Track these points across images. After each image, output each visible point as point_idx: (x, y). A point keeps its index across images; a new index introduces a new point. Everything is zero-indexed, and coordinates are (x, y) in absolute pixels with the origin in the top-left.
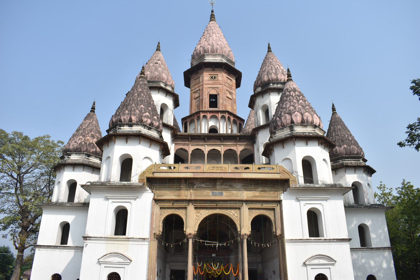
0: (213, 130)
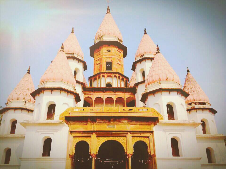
0: (109, 85)
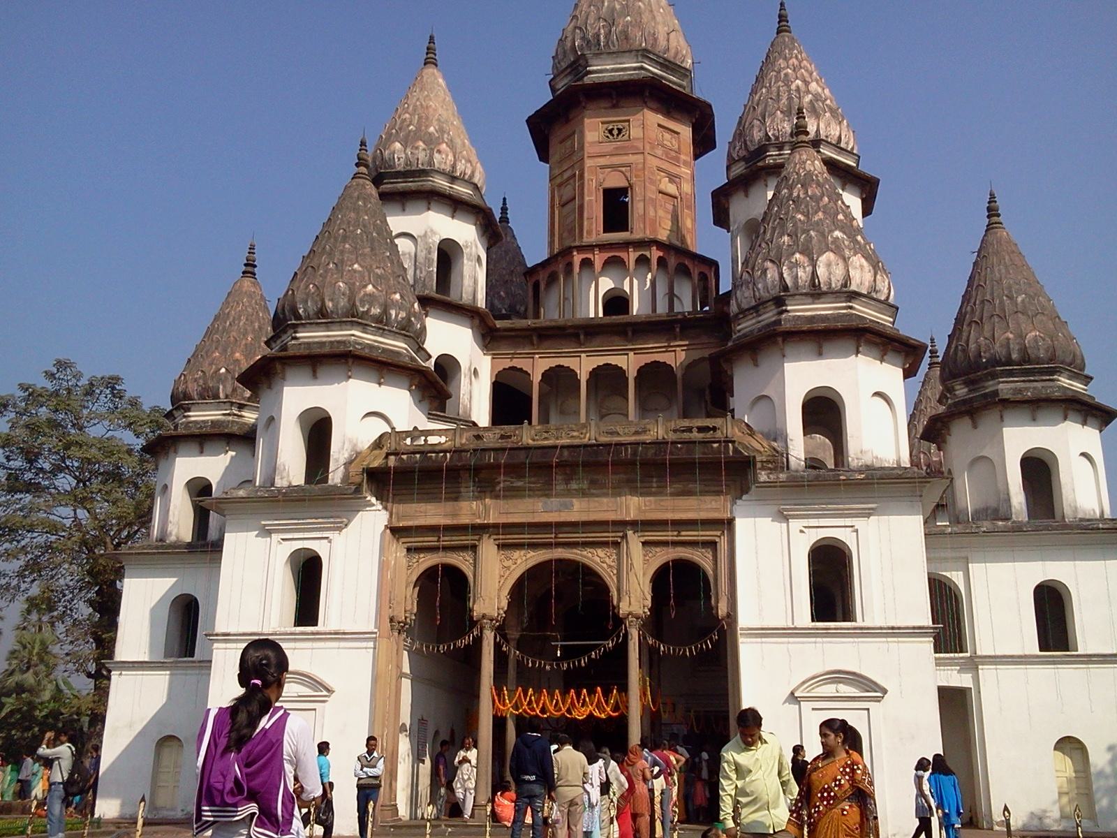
0: (616, 303)
